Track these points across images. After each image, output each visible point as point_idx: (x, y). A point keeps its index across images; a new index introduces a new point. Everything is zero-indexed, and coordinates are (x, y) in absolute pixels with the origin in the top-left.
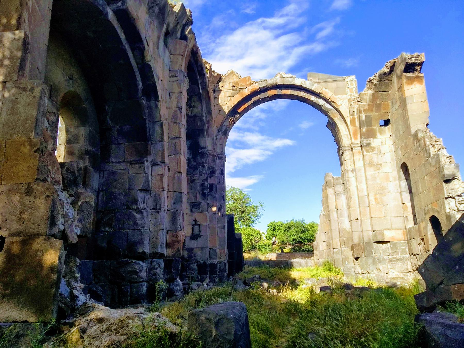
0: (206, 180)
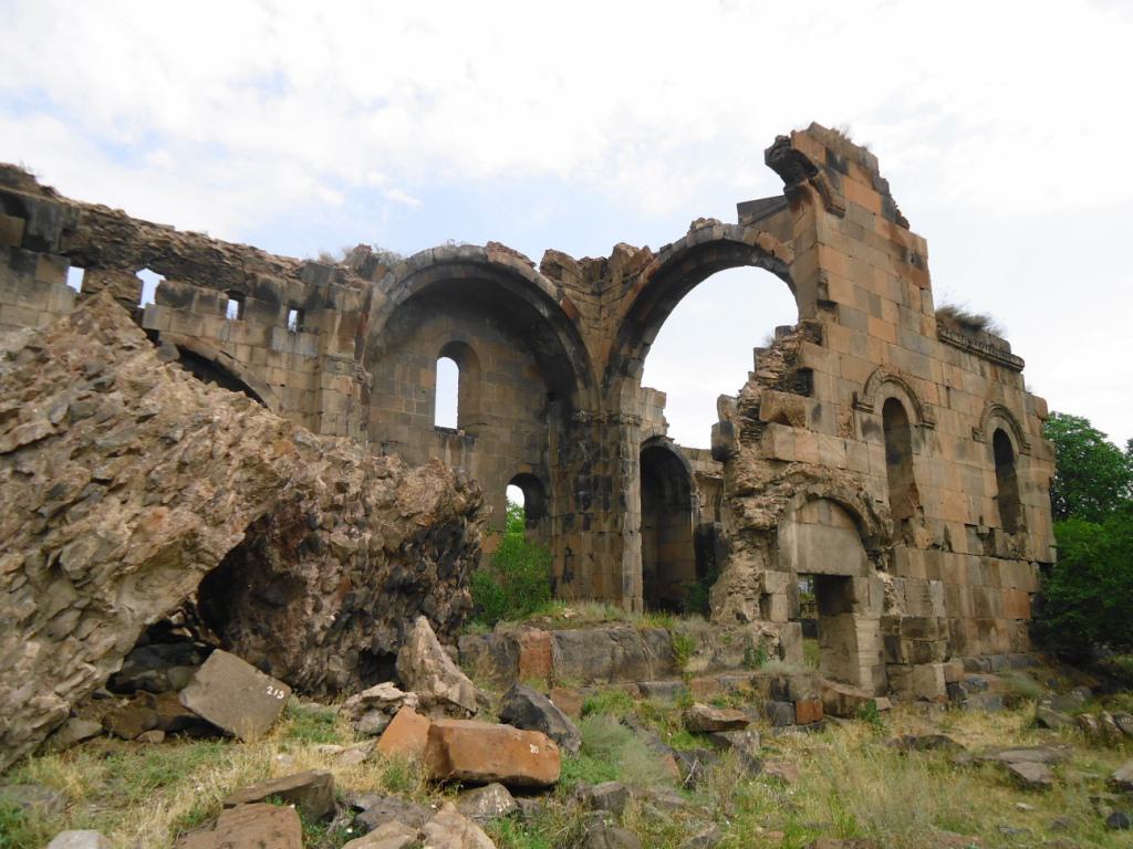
0: (586, 470)
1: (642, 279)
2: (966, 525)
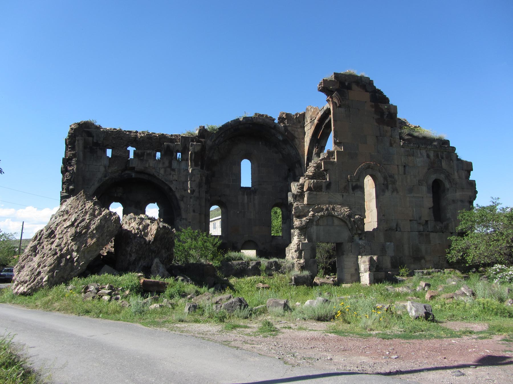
1: (316, 122)
2: (410, 220)
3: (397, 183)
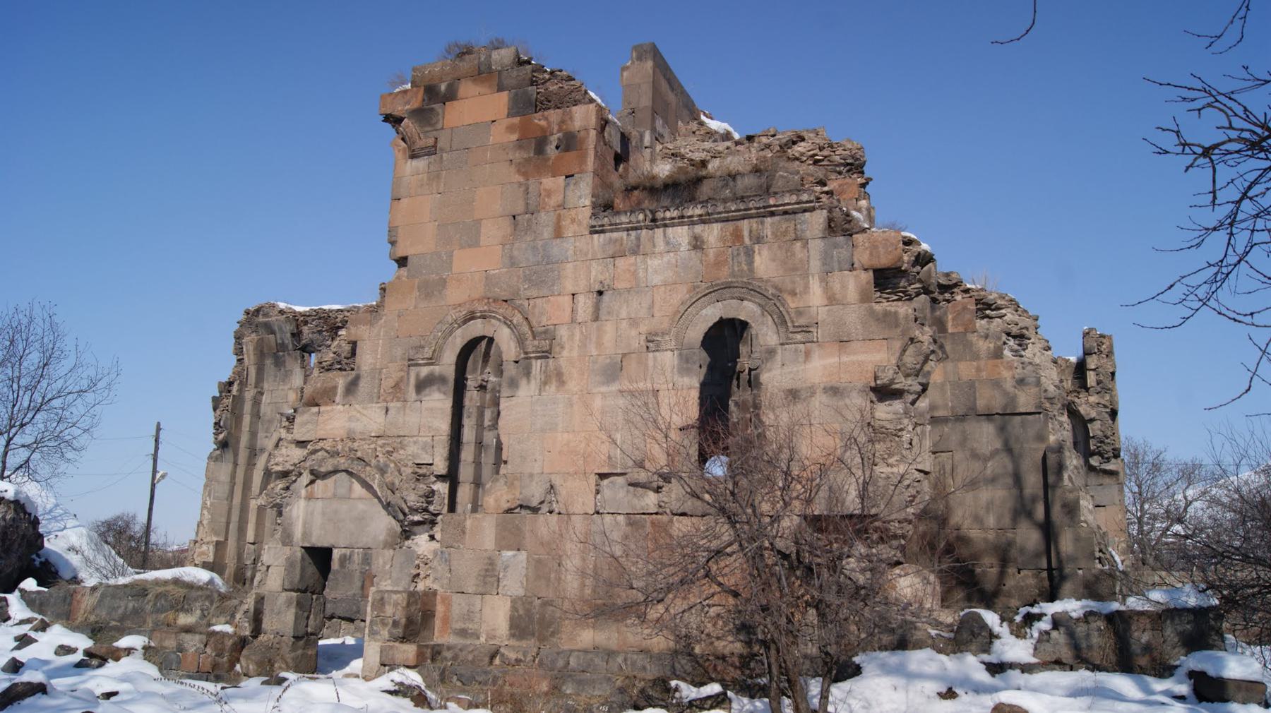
2: (603, 476)
3: (565, 353)
